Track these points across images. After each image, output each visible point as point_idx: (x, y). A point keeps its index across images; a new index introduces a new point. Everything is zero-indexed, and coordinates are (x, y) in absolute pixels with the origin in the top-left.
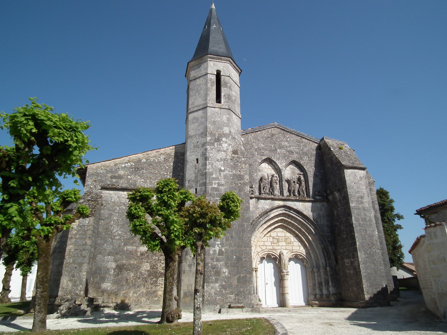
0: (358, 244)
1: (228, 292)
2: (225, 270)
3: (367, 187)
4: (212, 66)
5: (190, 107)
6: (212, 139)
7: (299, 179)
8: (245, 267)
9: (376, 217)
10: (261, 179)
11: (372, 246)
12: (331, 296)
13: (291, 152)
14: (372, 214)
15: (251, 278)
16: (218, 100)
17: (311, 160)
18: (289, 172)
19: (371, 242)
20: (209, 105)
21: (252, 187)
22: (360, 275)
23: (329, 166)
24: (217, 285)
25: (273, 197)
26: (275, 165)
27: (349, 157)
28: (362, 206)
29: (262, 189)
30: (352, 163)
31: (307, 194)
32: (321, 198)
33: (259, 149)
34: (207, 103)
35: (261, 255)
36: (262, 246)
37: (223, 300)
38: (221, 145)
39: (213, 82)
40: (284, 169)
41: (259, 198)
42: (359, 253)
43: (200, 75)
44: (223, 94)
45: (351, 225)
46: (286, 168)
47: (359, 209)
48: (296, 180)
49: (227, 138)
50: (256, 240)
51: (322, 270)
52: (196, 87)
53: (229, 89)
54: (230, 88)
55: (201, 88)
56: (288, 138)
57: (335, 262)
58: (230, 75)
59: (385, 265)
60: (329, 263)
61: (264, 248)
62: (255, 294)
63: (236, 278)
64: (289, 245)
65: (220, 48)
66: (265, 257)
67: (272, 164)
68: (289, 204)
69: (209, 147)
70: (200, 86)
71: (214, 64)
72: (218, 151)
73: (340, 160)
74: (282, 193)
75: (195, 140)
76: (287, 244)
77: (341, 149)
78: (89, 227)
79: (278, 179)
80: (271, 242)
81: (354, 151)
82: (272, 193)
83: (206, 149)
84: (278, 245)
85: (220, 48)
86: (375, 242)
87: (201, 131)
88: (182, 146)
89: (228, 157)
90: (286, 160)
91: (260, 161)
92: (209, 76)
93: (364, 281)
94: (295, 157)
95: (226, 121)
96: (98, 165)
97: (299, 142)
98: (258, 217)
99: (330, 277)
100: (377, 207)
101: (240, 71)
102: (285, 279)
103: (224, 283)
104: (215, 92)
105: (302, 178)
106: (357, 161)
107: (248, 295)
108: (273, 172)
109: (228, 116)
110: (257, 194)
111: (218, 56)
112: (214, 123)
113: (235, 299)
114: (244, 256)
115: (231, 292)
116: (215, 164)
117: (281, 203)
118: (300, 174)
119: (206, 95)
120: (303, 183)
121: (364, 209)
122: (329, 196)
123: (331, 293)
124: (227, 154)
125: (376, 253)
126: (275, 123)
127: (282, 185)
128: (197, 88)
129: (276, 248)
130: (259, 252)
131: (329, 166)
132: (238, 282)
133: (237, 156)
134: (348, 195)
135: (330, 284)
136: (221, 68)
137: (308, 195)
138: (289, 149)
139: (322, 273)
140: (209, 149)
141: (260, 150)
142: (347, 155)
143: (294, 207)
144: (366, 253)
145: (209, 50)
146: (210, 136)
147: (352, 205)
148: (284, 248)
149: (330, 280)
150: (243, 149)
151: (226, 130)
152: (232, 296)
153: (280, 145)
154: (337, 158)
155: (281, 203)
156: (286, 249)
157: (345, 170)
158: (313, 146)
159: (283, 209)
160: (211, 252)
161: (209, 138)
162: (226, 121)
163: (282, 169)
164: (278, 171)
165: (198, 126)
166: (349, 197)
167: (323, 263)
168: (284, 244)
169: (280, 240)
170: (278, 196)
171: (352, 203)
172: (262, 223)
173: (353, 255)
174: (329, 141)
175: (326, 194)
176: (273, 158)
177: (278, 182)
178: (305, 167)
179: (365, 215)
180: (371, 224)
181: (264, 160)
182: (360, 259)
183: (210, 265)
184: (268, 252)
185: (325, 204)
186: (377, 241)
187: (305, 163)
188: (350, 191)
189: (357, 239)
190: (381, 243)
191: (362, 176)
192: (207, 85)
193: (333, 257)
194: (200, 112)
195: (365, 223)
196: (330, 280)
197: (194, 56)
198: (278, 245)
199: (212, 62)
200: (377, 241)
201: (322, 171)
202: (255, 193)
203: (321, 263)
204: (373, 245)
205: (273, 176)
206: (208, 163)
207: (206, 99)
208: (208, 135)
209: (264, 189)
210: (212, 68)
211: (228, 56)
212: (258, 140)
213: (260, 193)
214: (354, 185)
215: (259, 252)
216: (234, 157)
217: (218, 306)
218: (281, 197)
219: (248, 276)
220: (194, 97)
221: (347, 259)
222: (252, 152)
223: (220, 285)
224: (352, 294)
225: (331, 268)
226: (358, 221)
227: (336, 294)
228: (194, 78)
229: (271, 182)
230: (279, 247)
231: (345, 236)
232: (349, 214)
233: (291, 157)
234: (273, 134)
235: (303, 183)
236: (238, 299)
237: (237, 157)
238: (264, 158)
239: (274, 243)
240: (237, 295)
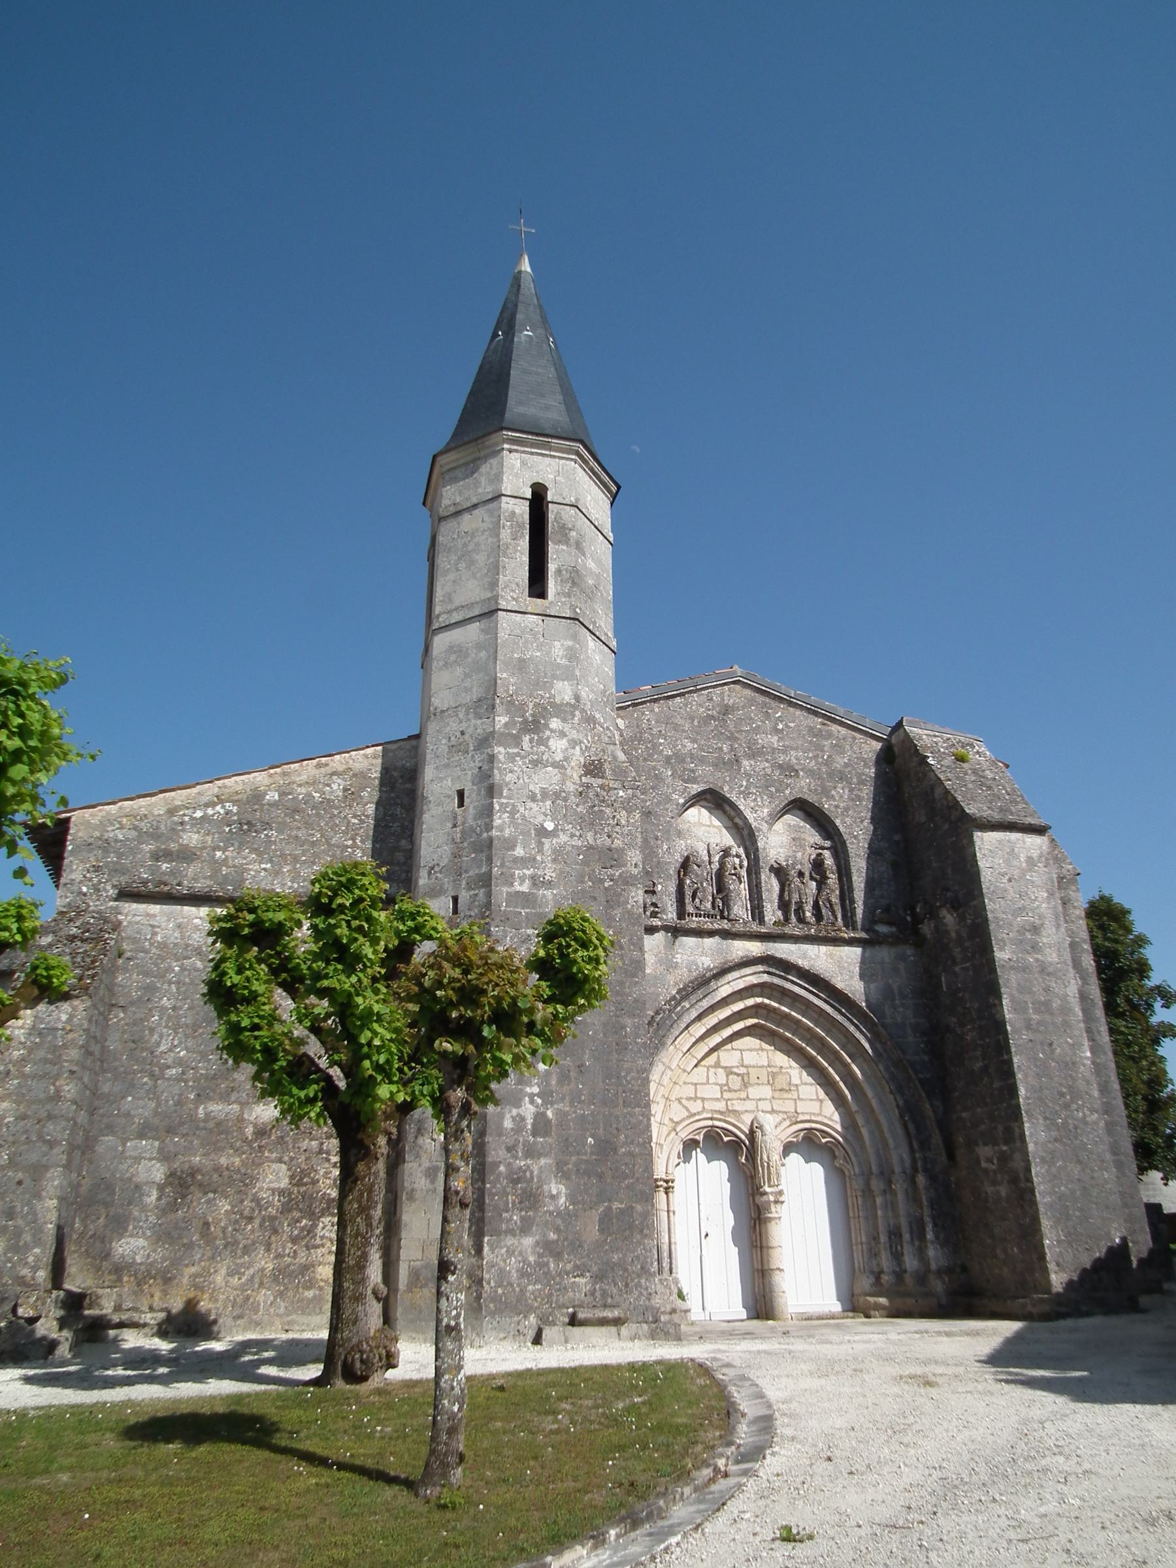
0: (1022, 1091)
1: (569, 1267)
2: (555, 1187)
3: (1051, 894)
4: (518, 469)
5: (437, 609)
6: (515, 723)
7: (818, 864)
8: (626, 1177)
9: (1083, 997)
10: (685, 865)
11: (1073, 1100)
12: (932, 1277)
13: (790, 770)
14: (1072, 990)
15: (649, 1215)
16: (537, 584)
17: (860, 799)
18: (784, 840)
19: (1070, 1087)
20: (503, 604)
21: (654, 892)
22: (1034, 1203)
23: (923, 819)
24: (528, 1241)
25: (725, 925)
26: (732, 813)
27: (989, 788)
28: (1037, 960)
29: (688, 900)
30: (1001, 810)
31: (844, 917)
32: (894, 929)
33: (679, 758)
34: (496, 598)
35: (684, 1134)
36: (689, 1099)
37: (551, 1295)
38: (543, 742)
39: (521, 526)
40: (765, 827)
41: (676, 932)
42: (1026, 1125)
43: (475, 500)
44: (552, 567)
45: (999, 1026)
46: (771, 825)
47: (1025, 969)
48: (807, 869)
49: (564, 720)
50: (666, 1080)
51: (899, 1186)
52: (460, 543)
53: (574, 551)
54: (578, 546)
55: (478, 544)
56: (780, 719)
57: (944, 1158)
58: (577, 500)
59: (1119, 1165)
60: (925, 1159)
61: (696, 1107)
62: (666, 1275)
63: (595, 1214)
64: (785, 1097)
65: (547, 408)
66: (700, 1138)
67: (725, 812)
68: (783, 950)
69: (501, 749)
70: (473, 536)
71: (523, 463)
72: (536, 763)
73: (959, 798)
74: (757, 911)
75: (453, 726)
76: (777, 1095)
77: (961, 759)
78: (70, 1036)
79: (745, 863)
80: (721, 1086)
81: (1007, 766)
82: (722, 912)
83: (492, 758)
84: (743, 1095)
85: (547, 408)
86: (1081, 1084)
87: (476, 693)
88: (407, 745)
89: (570, 787)
90: (771, 796)
91: (682, 801)
92: (507, 504)
93: (1046, 1223)
94: (803, 787)
95: (564, 662)
96: (108, 813)
97: (818, 734)
98: (674, 998)
99: (927, 1212)
100: (1088, 962)
101: (614, 489)
102: (770, 1219)
103: (553, 1236)
104: (526, 559)
105: (829, 861)
106: (1017, 803)
107: (639, 1276)
108: (728, 840)
109: (570, 643)
110: (671, 915)
111: (540, 435)
112: (521, 666)
113: (593, 1293)
114: (622, 1137)
115: (576, 1267)
116: (522, 809)
117: (755, 948)
118: (823, 848)
119: (496, 568)
120: (833, 879)
121: (1043, 969)
122: (922, 923)
123: (933, 1266)
124: (564, 774)
125: (1086, 1123)
126: (736, 667)
127: (758, 885)
128: (465, 545)
129: (738, 1106)
130: (678, 1123)
131: (923, 819)
132: (601, 1230)
133: (600, 781)
134: (986, 920)
135: (930, 1236)
136: (547, 479)
137: (849, 922)
138: (781, 759)
139: (901, 1197)
140: (501, 757)
141: (683, 761)
142: (982, 781)
143: (800, 963)
144: (1050, 1123)
145: (507, 415)
146: (508, 712)
147: (1002, 955)
148: (765, 1106)
149: (927, 1219)
150: (621, 756)
151: (563, 691)
152: (581, 1281)
153: (751, 744)
154: (947, 792)
155: (755, 948)
156: (773, 1111)
157: (978, 836)
158: (866, 748)
159: (760, 968)
160: (508, 1124)
161: (501, 720)
162: (564, 662)
163: (759, 830)
164: (745, 834)
165: (466, 676)
166: (992, 927)
167: (902, 1161)
168: (767, 1091)
169: (753, 1080)
170: (745, 923)
171: (1002, 949)
172: (687, 1019)
173: (1008, 1131)
174: (922, 734)
175: (913, 914)
177: (744, 873)
178: (838, 822)
179: (1047, 990)
180: (1066, 1024)
181: (695, 796)
182: (1031, 1147)
183: (502, 1168)
184: (710, 1123)
185: (909, 951)
186: (1088, 1082)
187: (837, 807)
188: (994, 907)
189: (1019, 1076)
190: (1104, 1089)
191: (1035, 854)
192: (498, 535)
193: (937, 1139)
194: (475, 627)
195: (1048, 1018)
196: (927, 1219)
197: (455, 435)
198: (743, 1095)
199: (517, 455)
200: (1088, 1082)
201: (897, 837)
202: (664, 911)
203: (895, 1160)
204: (1075, 1094)
205: (726, 852)
206: (497, 807)
207: (494, 584)
208: (499, 709)
209: (694, 896)
210: (516, 475)
211: (573, 435)
212: (676, 728)
213: (682, 914)
214: (1008, 886)
215: (678, 1123)
216: (588, 786)
217: (532, 1319)
218: (755, 927)
219: (639, 1208)
220: (451, 576)
221: (985, 1144)
222: (654, 768)
223: (537, 1243)
224: (1006, 1270)
225: (932, 1178)
226: (1024, 1010)
227: (949, 1271)
228: (452, 509)
229: (720, 875)
230: (750, 1105)
231: (979, 1065)
232: (990, 988)
233: (788, 785)
234: (727, 706)
235: (833, 879)
236: (604, 1293)
237: (602, 787)
238: (696, 788)
239: (730, 1090)
240: (599, 1277)
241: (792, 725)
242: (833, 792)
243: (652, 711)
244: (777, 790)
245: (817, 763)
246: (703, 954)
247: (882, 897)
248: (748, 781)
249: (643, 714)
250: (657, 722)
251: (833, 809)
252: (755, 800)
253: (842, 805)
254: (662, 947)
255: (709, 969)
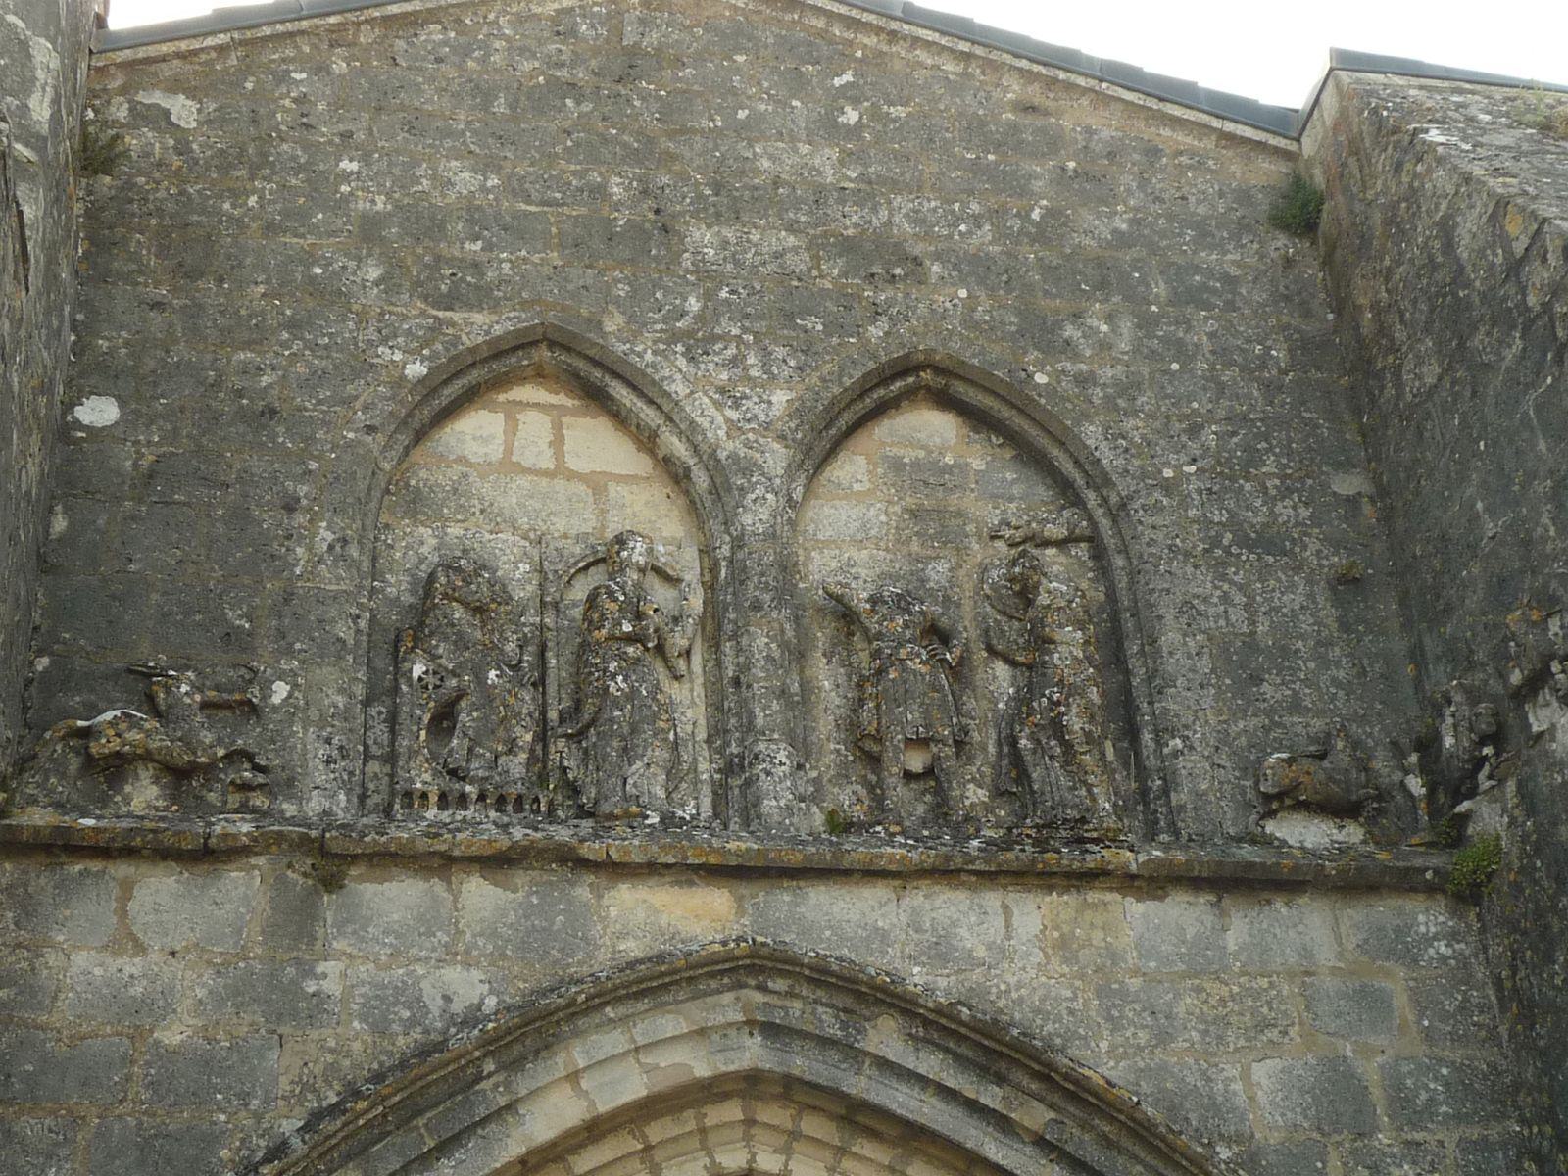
32: (1353, 833)
56: (852, 95)
67: (620, 418)
68: (842, 920)
79: (696, 602)
105: (1062, 577)
117: (702, 916)
138: (851, 220)
155: (702, 916)
159: (727, 1007)
176: (613, 323)
185: (1428, 918)
187: (1084, 381)
201: (1347, 485)
202: (288, 785)
222: (310, 257)
234: (634, 51)
241: (898, 111)
242: (1070, 331)
243: (321, 69)
244: (834, 327)
245: (1001, 235)
246: (450, 955)
247: (1295, 706)
248: (708, 296)
249: (283, 78)
250: (336, 104)
251: (1066, 386)
252: (735, 362)
253: (1107, 373)
254: (253, 933)
255: (472, 1018)
